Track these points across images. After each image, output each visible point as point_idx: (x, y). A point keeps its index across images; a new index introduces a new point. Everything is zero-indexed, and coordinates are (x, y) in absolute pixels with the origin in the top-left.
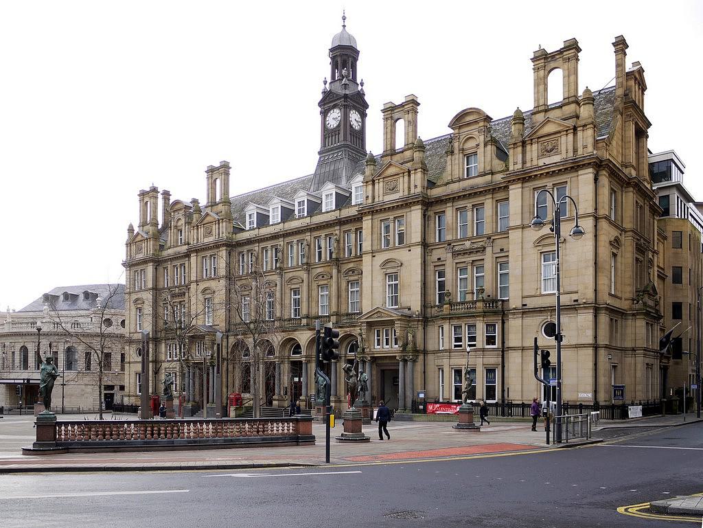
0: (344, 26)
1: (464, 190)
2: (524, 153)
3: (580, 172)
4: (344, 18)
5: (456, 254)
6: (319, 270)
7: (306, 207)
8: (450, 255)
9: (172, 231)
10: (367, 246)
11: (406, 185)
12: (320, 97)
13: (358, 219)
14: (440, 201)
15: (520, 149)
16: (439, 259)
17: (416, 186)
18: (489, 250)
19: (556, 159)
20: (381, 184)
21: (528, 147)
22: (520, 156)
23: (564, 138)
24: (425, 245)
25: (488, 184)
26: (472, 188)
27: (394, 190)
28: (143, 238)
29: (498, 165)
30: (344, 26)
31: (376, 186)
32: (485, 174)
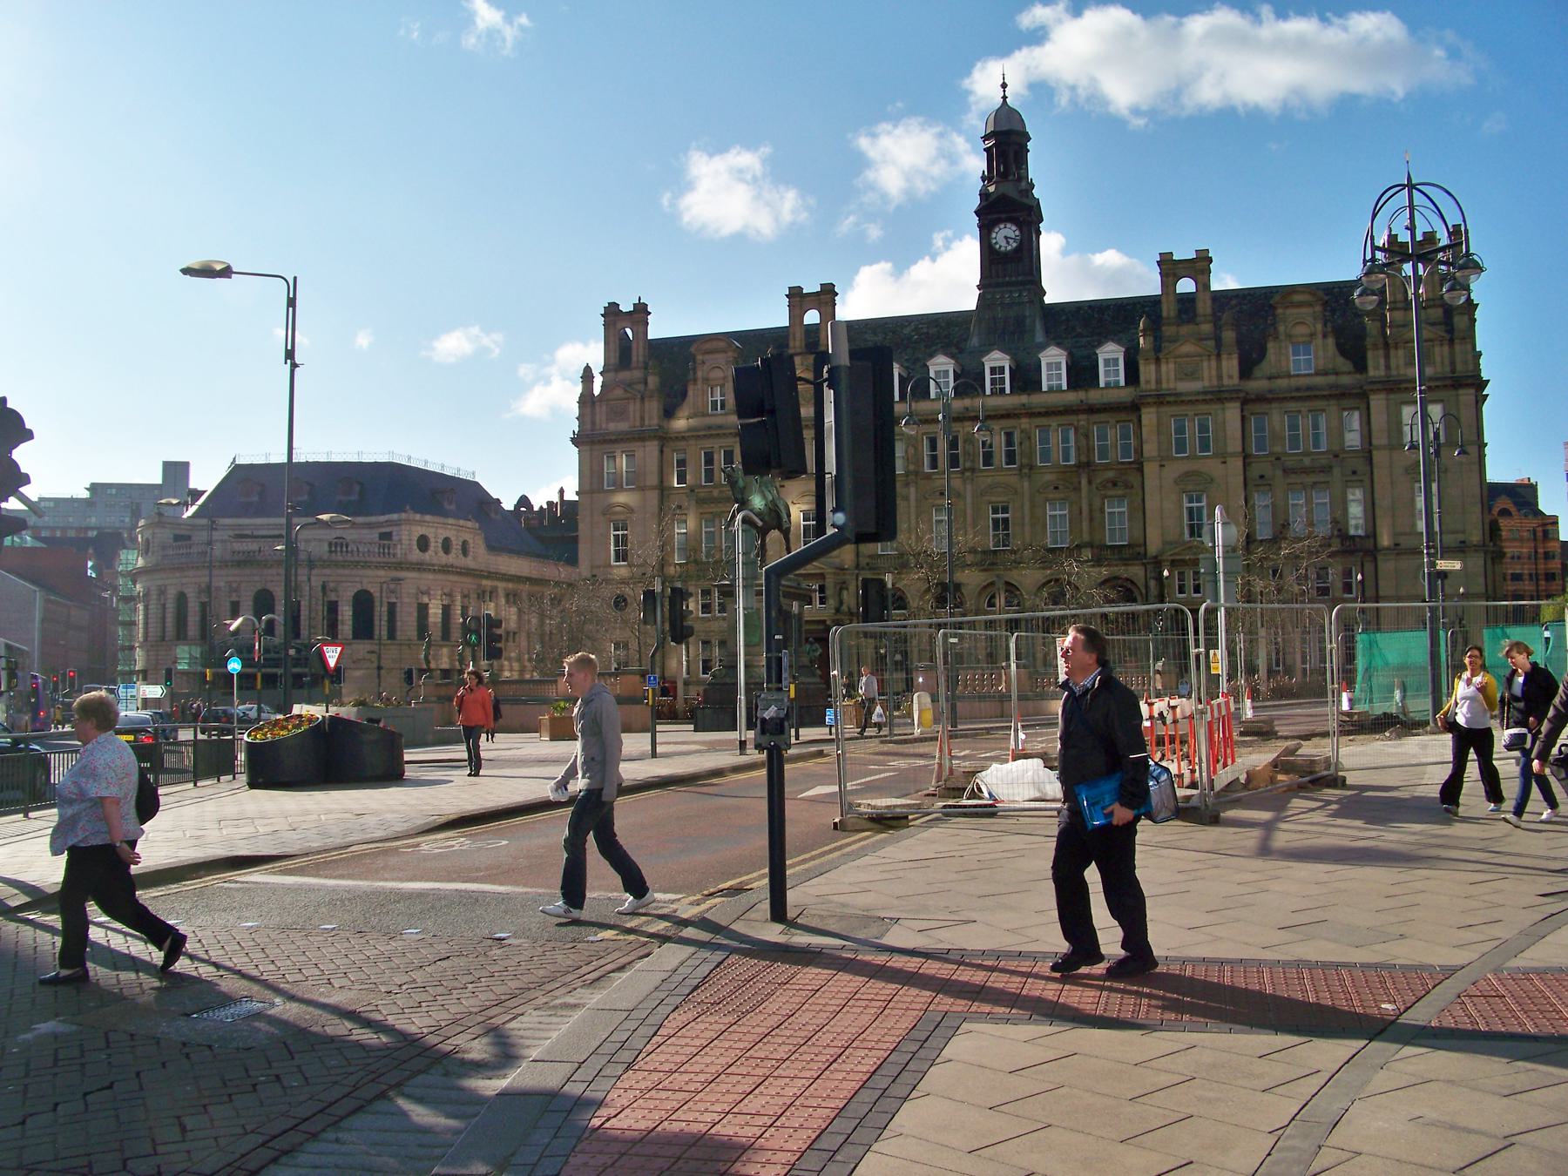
0: (1005, 98)
1: (1298, 389)
2: (1387, 357)
3: (1461, 391)
4: (1004, 86)
5: (1286, 471)
6: (1048, 477)
7: (1007, 375)
8: (1279, 473)
10: (1150, 449)
11: (1214, 373)
12: (976, 202)
14: (1261, 398)
15: (1381, 352)
16: (1262, 477)
17: (1230, 377)
18: (1337, 471)
20: (1172, 366)
21: (1392, 352)
22: (1382, 361)
23: (1437, 349)
24: (1246, 458)
25: (1331, 387)
26: (1309, 388)
27: (1192, 375)
29: (1343, 364)
30: (1005, 98)
31: (1164, 368)
32: (1326, 374)
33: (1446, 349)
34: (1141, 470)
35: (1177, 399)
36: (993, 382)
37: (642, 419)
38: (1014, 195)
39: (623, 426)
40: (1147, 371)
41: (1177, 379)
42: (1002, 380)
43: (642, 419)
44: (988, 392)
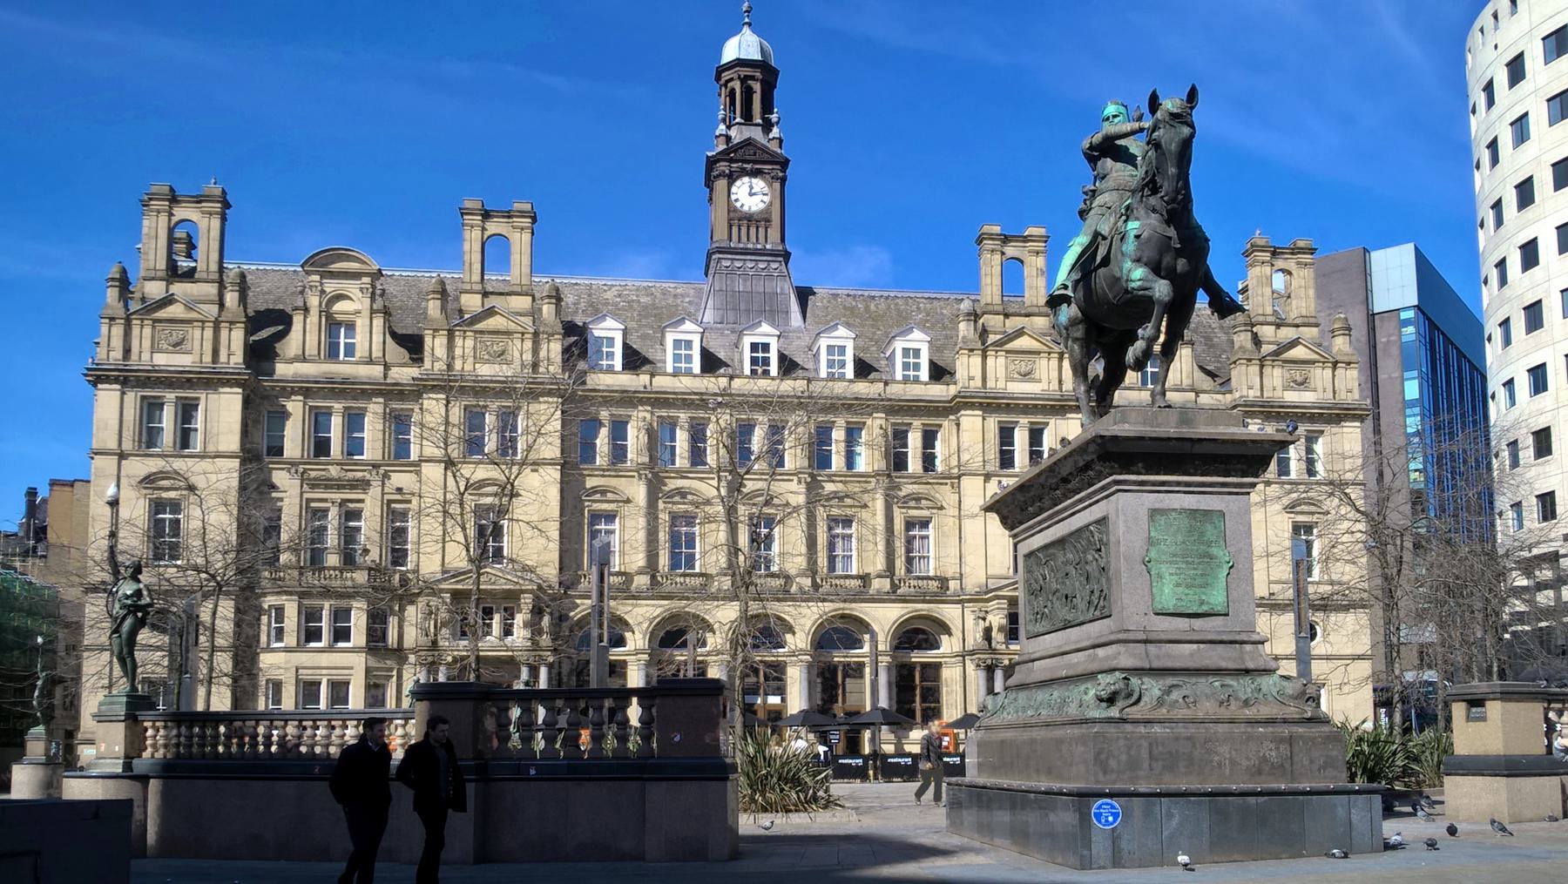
9: (313, 317)
11: (1055, 374)
13: (951, 408)
19: (1307, 397)
20: (1001, 360)
21: (1267, 370)
28: (193, 315)
31: (990, 361)
33: (1328, 372)
34: (957, 489)
35: (1010, 408)
36: (754, 361)
37: (216, 353)
38: (764, 141)
39: (183, 361)
40: (967, 368)
41: (1009, 379)
42: (766, 362)
43: (216, 353)
44: (747, 371)
